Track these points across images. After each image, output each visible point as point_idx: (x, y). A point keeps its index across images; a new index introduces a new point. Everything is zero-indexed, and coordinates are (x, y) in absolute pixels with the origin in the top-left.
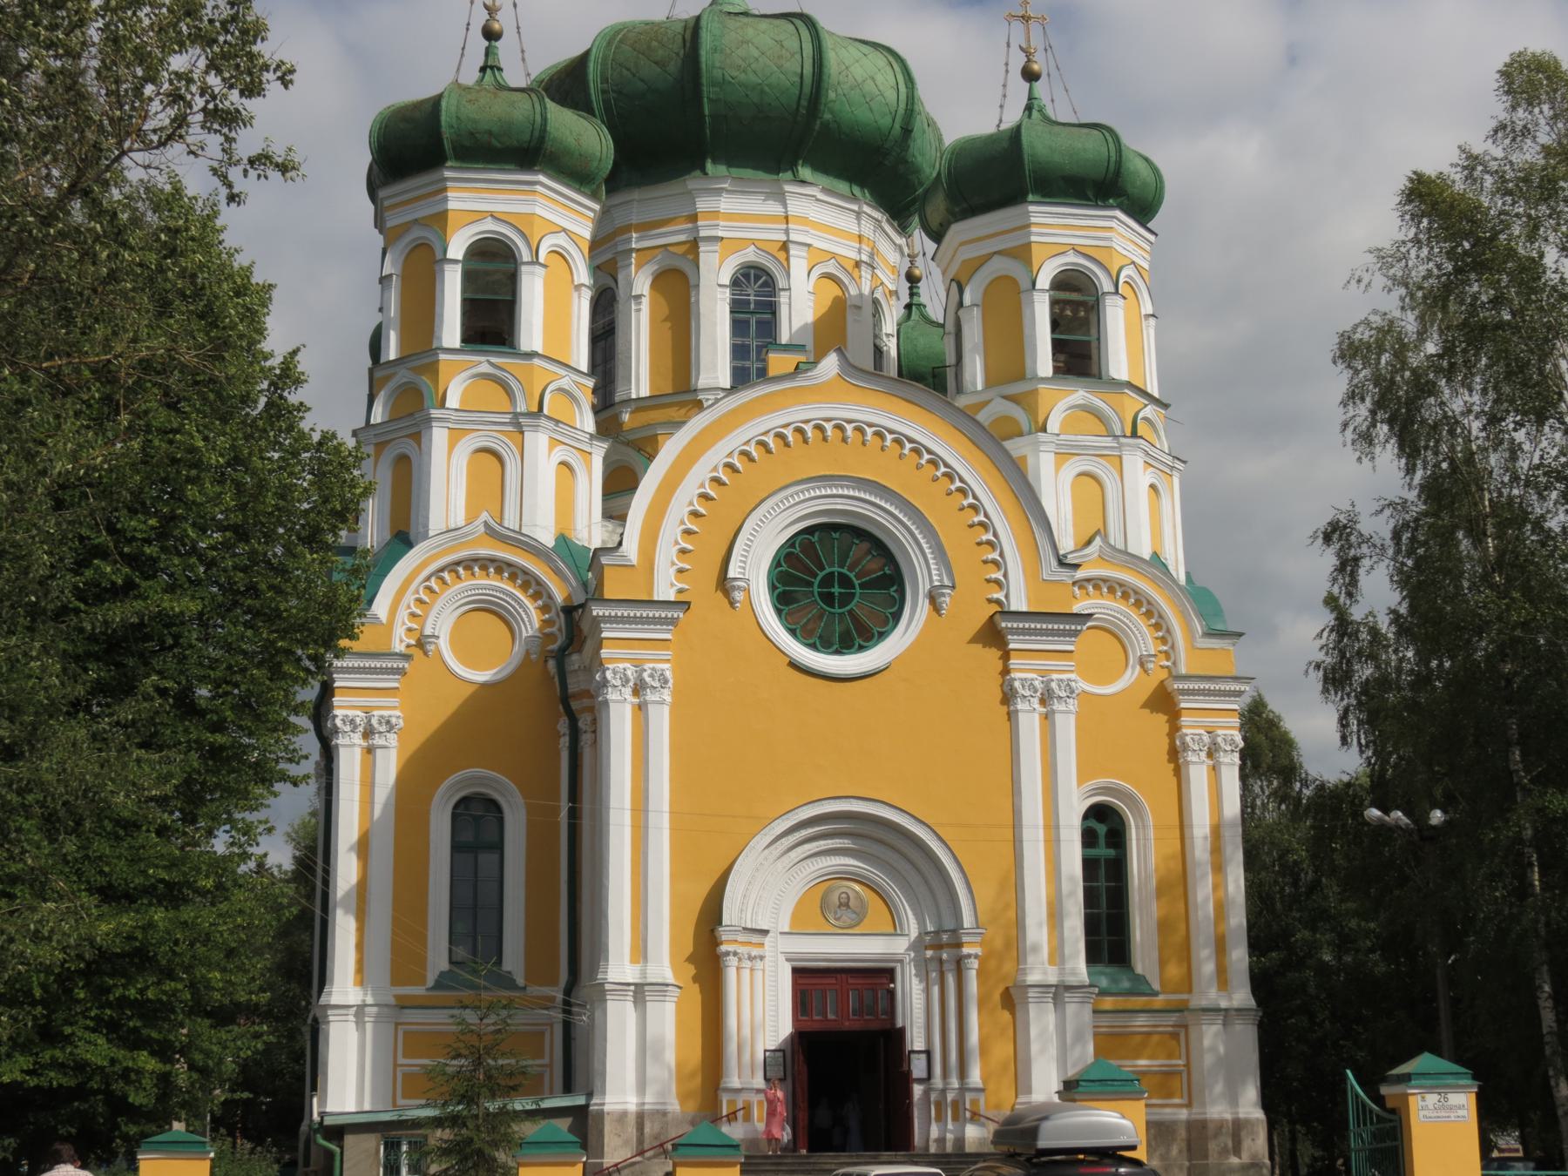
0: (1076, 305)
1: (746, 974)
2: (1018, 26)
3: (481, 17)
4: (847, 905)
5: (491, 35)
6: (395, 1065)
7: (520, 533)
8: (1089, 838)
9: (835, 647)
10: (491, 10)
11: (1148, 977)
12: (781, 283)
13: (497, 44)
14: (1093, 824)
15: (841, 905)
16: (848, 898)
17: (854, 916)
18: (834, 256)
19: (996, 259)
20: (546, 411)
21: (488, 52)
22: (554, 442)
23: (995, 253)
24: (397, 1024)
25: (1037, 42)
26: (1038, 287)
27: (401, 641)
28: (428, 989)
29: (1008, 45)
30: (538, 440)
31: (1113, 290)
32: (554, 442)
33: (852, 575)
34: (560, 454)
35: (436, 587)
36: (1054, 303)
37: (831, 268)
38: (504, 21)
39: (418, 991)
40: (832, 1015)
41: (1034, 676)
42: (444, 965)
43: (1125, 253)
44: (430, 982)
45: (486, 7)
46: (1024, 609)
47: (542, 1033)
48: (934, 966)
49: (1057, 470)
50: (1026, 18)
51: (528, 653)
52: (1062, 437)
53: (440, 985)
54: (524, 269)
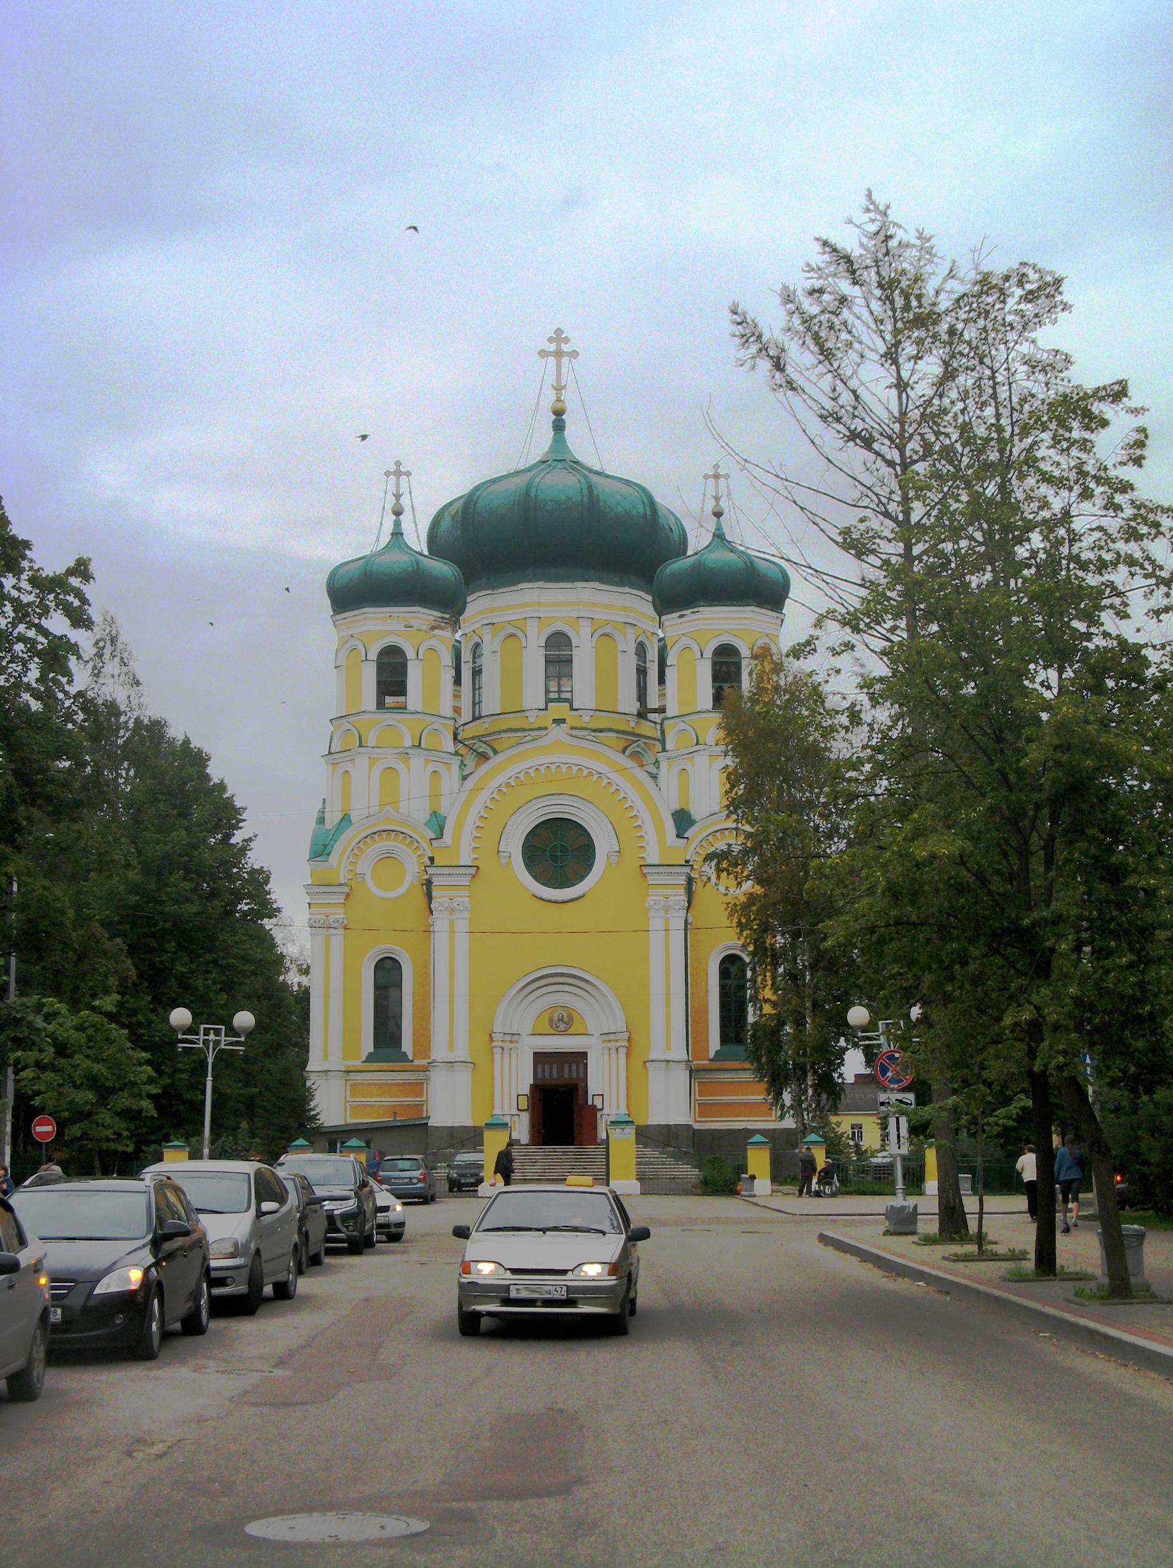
1: (506, 1057)
2: (711, 481)
3: (391, 501)
4: (562, 1020)
5: (398, 513)
6: (346, 1102)
7: (409, 816)
8: (724, 973)
10: (398, 496)
12: (574, 645)
13: (401, 517)
14: (727, 965)
15: (559, 1020)
18: (608, 622)
20: (423, 745)
21: (397, 524)
22: (427, 761)
24: (346, 1080)
25: (723, 491)
30: (417, 761)
32: (427, 761)
34: (432, 767)
35: (362, 846)
36: (714, 664)
37: (606, 630)
38: (405, 502)
39: (357, 1063)
40: (553, 1074)
41: (662, 898)
42: (371, 1049)
45: (394, 495)
46: (657, 862)
47: (423, 1083)
50: (716, 477)
51: (413, 882)
53: (370, 1058)
54: (409, 663)
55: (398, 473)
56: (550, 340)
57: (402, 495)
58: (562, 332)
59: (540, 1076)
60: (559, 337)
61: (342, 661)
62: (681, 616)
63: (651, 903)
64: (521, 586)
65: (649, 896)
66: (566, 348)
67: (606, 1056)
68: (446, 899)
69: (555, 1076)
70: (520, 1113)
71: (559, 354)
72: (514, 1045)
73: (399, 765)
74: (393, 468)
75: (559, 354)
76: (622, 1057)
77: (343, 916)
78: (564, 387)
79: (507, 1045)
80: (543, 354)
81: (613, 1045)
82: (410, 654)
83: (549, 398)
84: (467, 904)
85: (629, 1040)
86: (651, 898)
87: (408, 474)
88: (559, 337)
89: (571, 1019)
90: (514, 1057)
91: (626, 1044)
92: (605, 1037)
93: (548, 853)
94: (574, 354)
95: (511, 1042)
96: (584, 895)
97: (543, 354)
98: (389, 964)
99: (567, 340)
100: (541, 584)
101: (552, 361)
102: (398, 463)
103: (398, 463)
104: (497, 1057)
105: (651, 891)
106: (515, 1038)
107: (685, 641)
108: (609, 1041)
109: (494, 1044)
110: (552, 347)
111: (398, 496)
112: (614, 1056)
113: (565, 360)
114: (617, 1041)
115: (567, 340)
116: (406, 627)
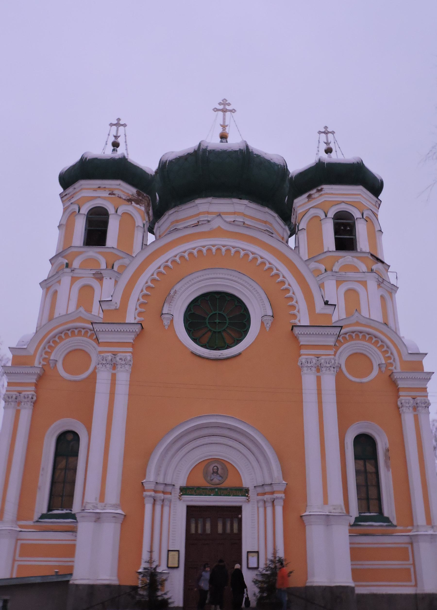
0: (345, 225)
1: (158, 508)
2: (323, 136)
3: (112, 139)
4: (217, 473)
9: (216, 347)
10: (116, 137)
11: (391, 519)
15: (214, 472)
16: (218, 469)
17: (220, 478)
19: (311, 209)
23: (311, 208)
26: (328, 217)
27: (40, 363)
28: (34, 522)
29: (319, 142)
31: (361, 217)
33: (225, 315)
38: (120, 140)
43: (366, 205)
44: (36, 518)
48: (261, 504)
49: (337, 288)
50: (326, 133)
52: (340, 273)
54: (110, 217)
55: (118, 125)
56: (220, 104)
57: (119, 137)
58: (226, 100)
59: (193, 531)
60: (224, 103)
61: (64, 222)
62: (309, 197)
63: (304, 361)
64: (198, 201)
65: (300, 356)
66: (228, 107)
67: (261, 510)
68: (109, 354)
69: (208, 530)
70: (170, 571)
71: (224, 111)
72: (168, 496)
73: (95, 284)
74: (115, 122)
75: (224, 111)
76: (279, 510)
77: (33, 393)
78: (227, 126)
79: (161, 495)
80: (216, 110)
81: (267, 497)
82: (111, 210)
83: (220, 130)
84: (129, 358)
85: (285, 492)
86: (302, 357)
87: (124, 125)
88: (224, 103)
89: (225, 469)
90: (166, 509)
91: (283, 495)
92: (260, 490)
93: (207, 321)
94: (233, 111)
95: (164, 493)
96: (240, 354)
97: (216, 110)
98: (70, 437)
99: (229, 104)
100: (210, 199)
101: (221, 113)
102: (119, 120)
103: (119, 120)
104: (148, 507)
105: (303, 351)
106: (169, 489)
107: (312, 212)
108: (264, 494)
109: (145, 493)
110: (221, 107)
111: (116, 137)
112: (269, 510)
113: (228, 114)
114: (273, 493)
115: (229, 104)
116: (110, 194)
